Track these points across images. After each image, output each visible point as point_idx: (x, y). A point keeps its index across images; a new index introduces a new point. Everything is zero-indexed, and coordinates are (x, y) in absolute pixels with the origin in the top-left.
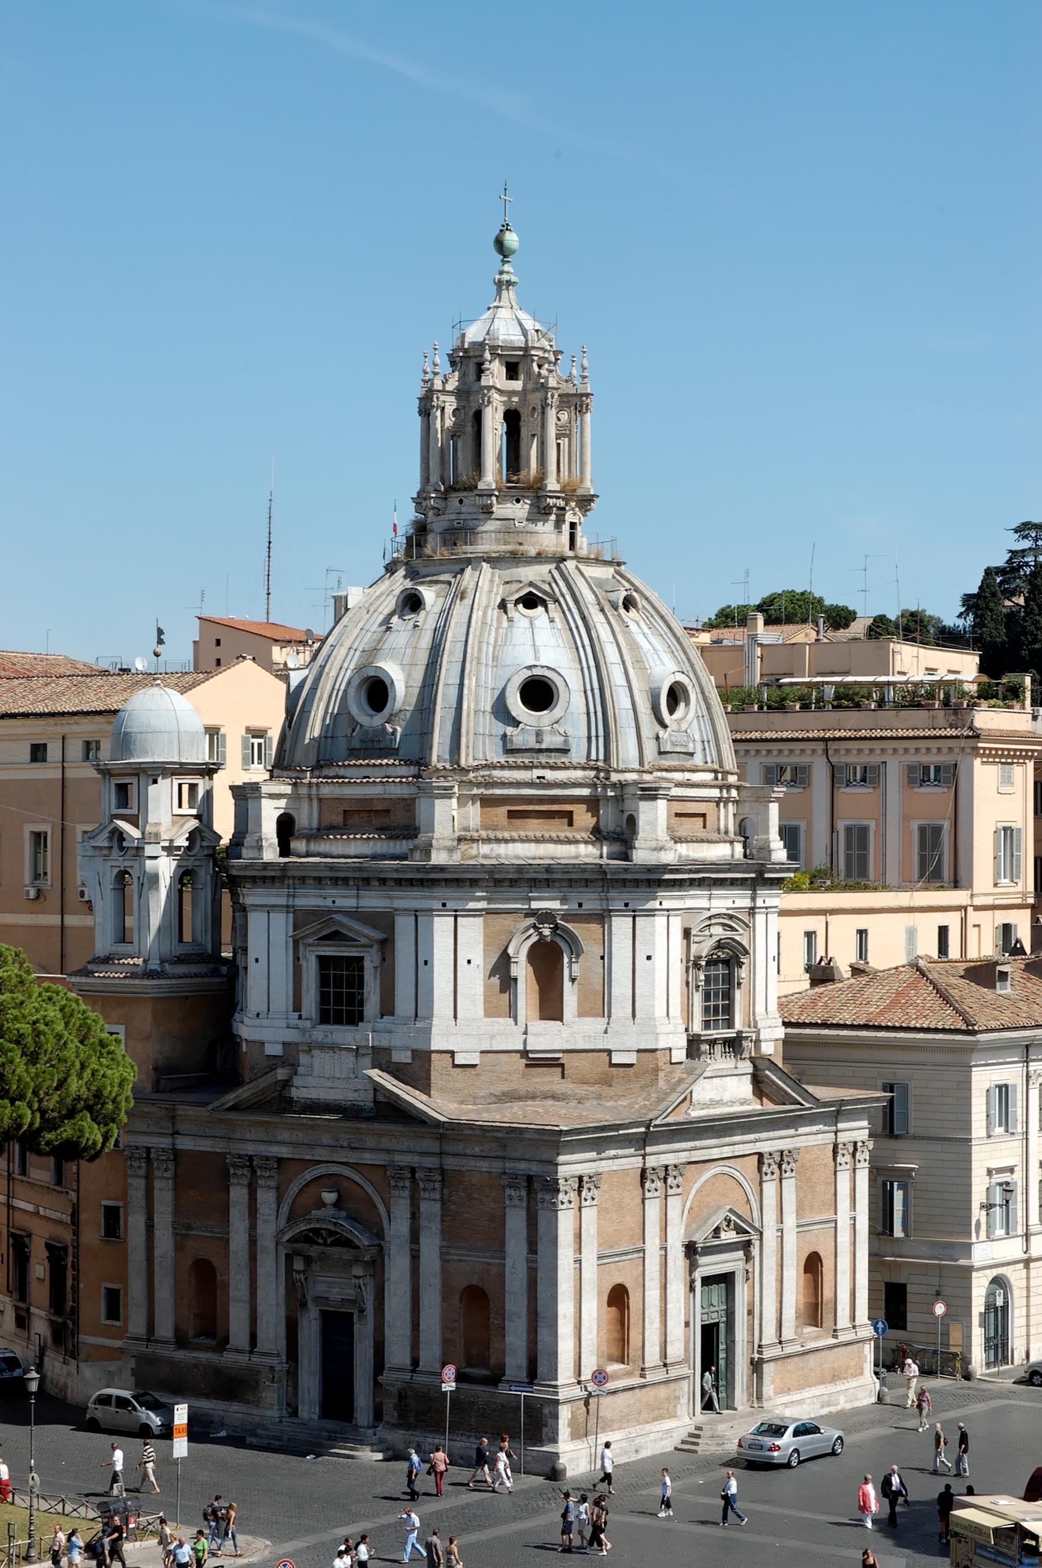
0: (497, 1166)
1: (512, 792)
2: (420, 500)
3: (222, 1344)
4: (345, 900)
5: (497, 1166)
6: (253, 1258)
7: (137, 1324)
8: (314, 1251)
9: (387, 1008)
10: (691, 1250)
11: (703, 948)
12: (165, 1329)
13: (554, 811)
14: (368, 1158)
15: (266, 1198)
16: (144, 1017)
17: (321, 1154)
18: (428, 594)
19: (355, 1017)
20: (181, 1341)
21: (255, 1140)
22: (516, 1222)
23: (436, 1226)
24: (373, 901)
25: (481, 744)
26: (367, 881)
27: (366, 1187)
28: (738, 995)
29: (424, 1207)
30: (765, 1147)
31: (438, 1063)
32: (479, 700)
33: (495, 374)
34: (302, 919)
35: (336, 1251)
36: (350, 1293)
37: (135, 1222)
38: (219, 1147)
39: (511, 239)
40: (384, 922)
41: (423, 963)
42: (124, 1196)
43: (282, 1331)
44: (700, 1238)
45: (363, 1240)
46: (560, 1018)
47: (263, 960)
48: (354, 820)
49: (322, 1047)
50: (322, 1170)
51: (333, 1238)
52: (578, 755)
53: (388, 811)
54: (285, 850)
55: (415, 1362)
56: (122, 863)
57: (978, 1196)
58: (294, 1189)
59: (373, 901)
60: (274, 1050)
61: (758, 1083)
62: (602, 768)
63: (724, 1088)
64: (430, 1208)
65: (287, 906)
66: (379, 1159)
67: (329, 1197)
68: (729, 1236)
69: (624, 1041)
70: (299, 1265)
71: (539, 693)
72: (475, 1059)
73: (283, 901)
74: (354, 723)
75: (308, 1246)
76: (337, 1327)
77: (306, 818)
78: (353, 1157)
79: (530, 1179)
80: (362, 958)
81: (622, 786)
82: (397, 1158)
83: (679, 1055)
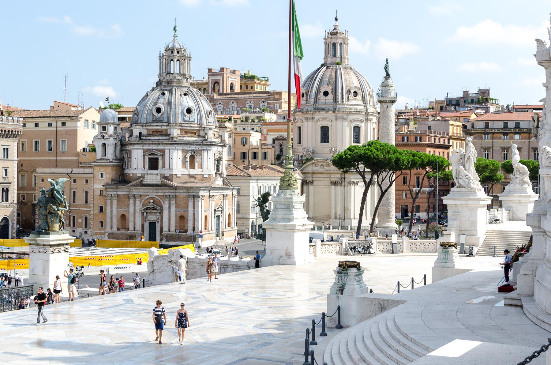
0: (187, 194)
1: (186, 128)
2: (160, 75)
3: (128, 229)
4: (155, 147)
5: (187, 194)
6: (135, 213)
7: (108, 227)
8: (149, 211)
9: (163, 167)
10: (215, 210)
11: (217, 157)
12: (115, 228)
13: (193, 132)
14: (160, 194)
15: (138, 202)
16: (109, 170)
17: (149, 194)
18: (166, 92)
19: (157, 168)
20: (118, 229)
21: (135, 192)
22: (191, 204)
23: (174, 205)
24: (161, 147)
25: (179, 120)
26: (159, 144)
28: (221, 166)
29: (171, 202)
30: (224, 194)
31: (174, 176)
32: (179, 111)
33: (175, 53)
34: (145, 151)
35: (154, 211)
36: (156, 219)
37: (108, 208)
39: (177, 28)
40: (163, 152)
41: (170, 158)
42: (106, 203)
43: (141, 226)
44: (216, 208)
45: (158, 208)
46: (194, 169)
49: (150, 174)
50: (150, 196)
51: (153, 208)
52: (196, 122)
54: (140, 139)
55: (169, 230)
56: (104, 142)
57: (251, 206)
58: (144, 200)
59: (161, 147)
60: (139, 175)
61: (223, 182)
62: (200, 125)
63: (219, 182)
64: (173, 202)
66: (162, 194)
67: (152, 201)
68: (220, 209)
69: (206, 173)
70: (145, 214)
71: (189, 111)
72: (180, 176)
75: (147, 210)
76: (152, 226)
77: (144, 132)
78: (157, 194)
79: (194, 196)
80: (158, 158)
81: (204, 127)
82: (166, 194)
83: (214, 176)
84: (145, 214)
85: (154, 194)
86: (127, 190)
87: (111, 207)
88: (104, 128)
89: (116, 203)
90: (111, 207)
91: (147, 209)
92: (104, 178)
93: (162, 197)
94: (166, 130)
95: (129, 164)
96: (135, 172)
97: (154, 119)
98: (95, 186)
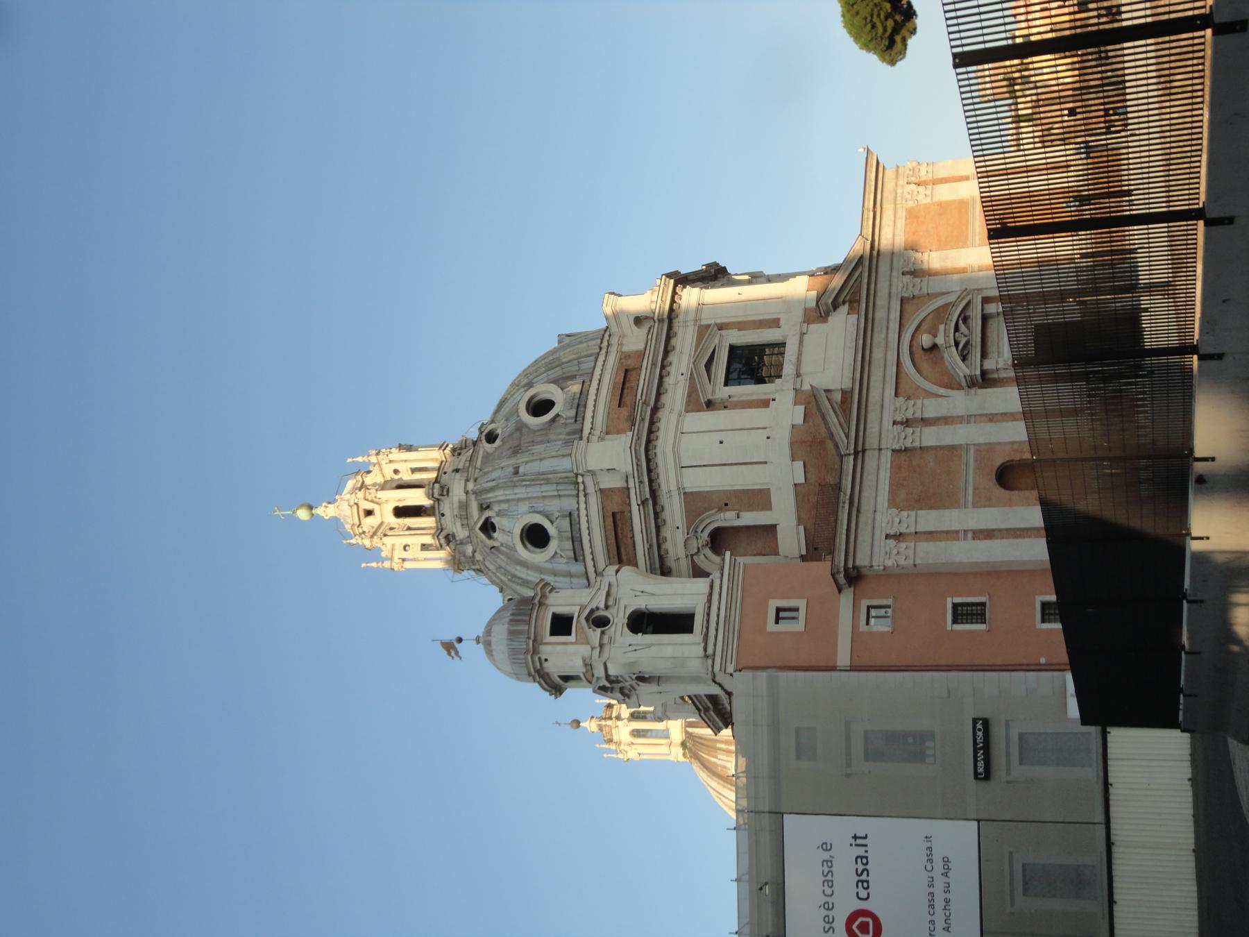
6: (992, 418)
9: (775, 323)
14: (895, 315)
15: (932, 408)
23: (953, 253)
27: (920, 318)
38: (886, 457)
47: (719, 436)
48: (627, 399)
53: (626, 371)
56: (619, 619)
65: (680, 415)
73: (674, 418)
74: (558, 415)
78: (894, 326)
80: (732, 348)
84: (989, 364)
85: (893, 336)
86: (871, 460)
87: (951, 535)
88: (562, 625)
89: (934, 513)
90: (951, 535)
91: (964, 358)
92: (801, 604)
93: (909, 308)
94: (626, 356)
95: (750, 518)
96: (783, 436)
97: (572, 413)
98: (843, 659)
